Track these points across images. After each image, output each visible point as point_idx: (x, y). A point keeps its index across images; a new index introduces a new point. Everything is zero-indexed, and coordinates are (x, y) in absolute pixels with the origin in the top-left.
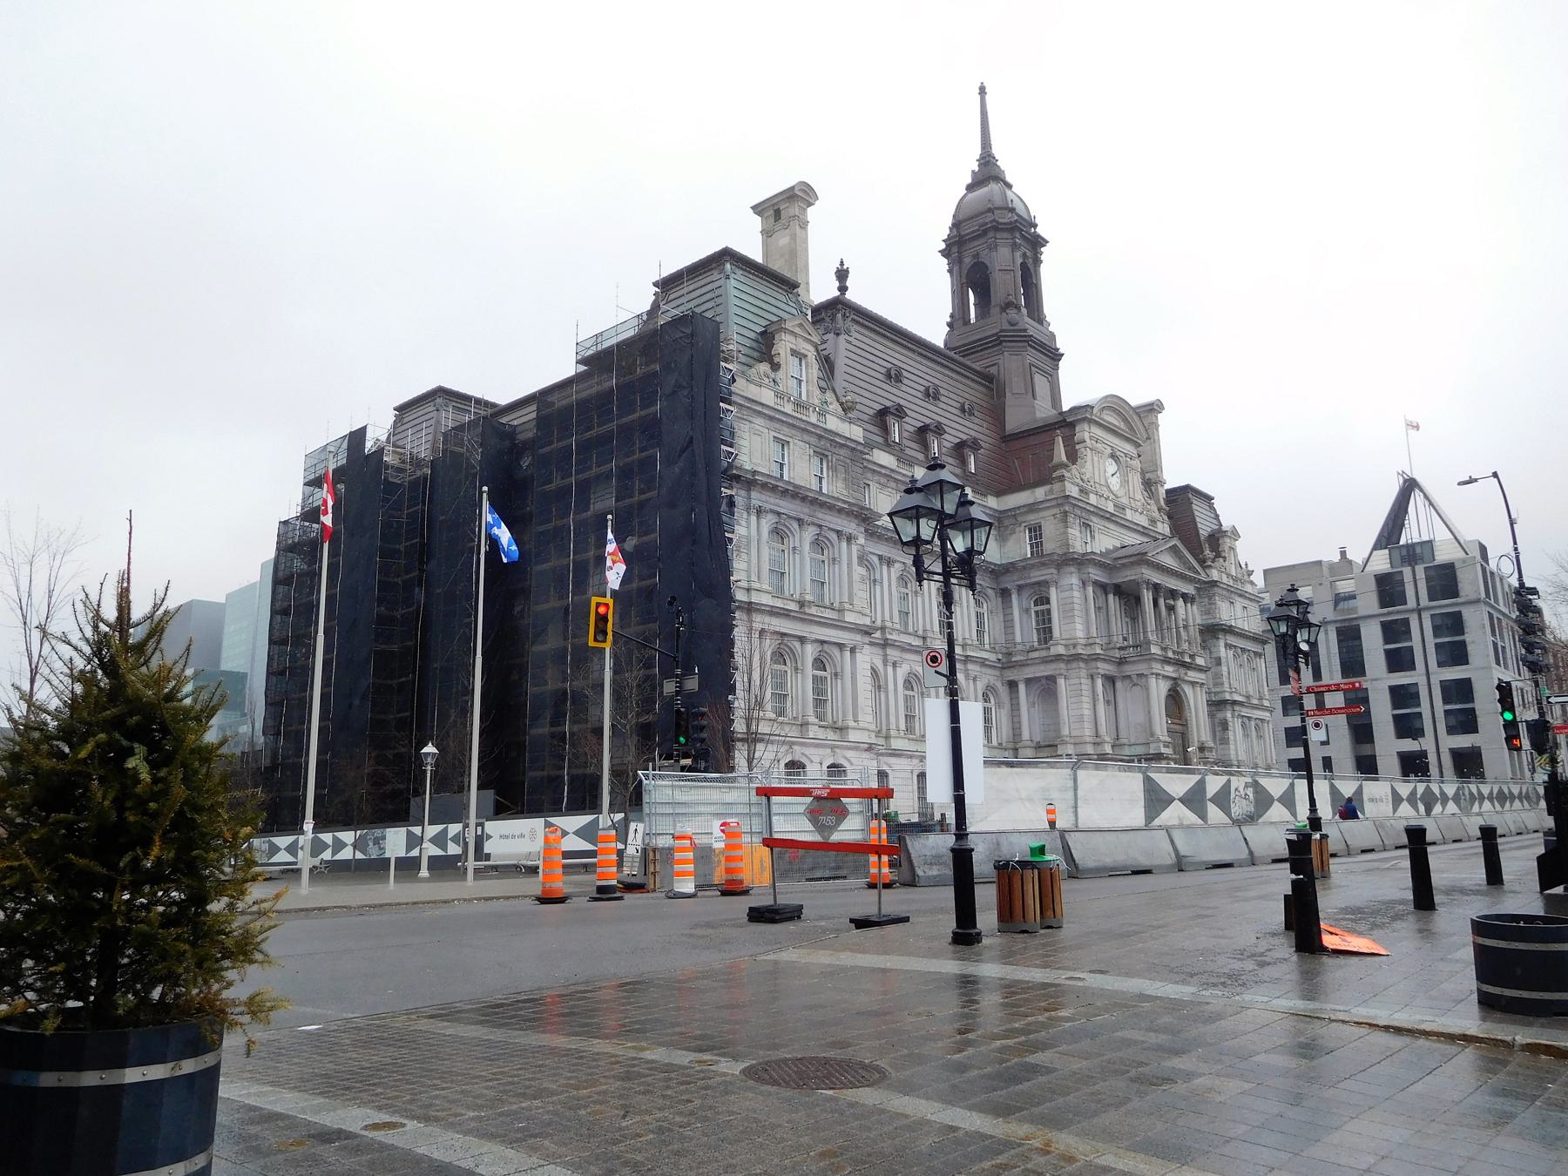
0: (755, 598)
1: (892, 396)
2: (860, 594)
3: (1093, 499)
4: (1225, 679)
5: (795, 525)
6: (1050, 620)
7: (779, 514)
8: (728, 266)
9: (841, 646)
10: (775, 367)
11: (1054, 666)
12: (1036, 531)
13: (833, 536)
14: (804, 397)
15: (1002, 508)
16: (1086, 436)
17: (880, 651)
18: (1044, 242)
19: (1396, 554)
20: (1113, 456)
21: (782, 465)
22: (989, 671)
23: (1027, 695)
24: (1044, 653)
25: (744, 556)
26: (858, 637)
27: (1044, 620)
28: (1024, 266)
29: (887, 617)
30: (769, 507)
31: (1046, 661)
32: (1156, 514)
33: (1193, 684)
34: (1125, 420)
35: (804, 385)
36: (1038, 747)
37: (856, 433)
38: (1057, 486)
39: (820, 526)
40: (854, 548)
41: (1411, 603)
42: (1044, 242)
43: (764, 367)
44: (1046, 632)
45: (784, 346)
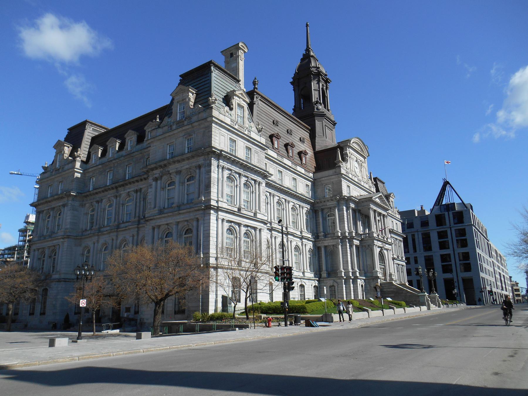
0: (220, 204)
1: (275, 130)
3: (350, 176)
5: (238, 175)
8: (212, 68)
9: (255, 229)
10: (231, 109)
16: (348, 152)
26: (262, 225)
28: (322, 89)
32: (371, 184)
33: (387, 250)
34: (361, 148)
37: (263, 140)
38: (337, 170)
39: (248, 177)
43: (227, 108)
45: (235, 101)
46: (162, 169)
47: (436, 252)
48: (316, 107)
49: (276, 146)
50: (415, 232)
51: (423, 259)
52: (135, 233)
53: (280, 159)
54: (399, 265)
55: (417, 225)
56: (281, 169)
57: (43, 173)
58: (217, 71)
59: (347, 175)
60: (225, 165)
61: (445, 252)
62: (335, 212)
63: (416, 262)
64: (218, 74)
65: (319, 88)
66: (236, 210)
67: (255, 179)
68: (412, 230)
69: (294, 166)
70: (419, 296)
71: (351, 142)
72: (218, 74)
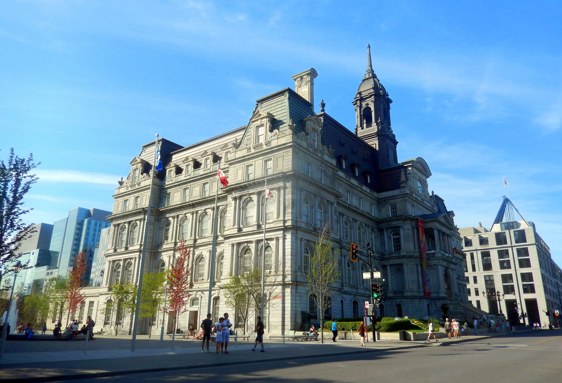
7: (308, 191)
11: (402, 260)
12: (394, 208)
15: (380, 197)
18: (391, 101)
19: (503, 226)
20: (420, 180)
21: (308, 172)
22: (376, 261)
23: (391, 271)
24: (398, 255)
27: (397, 242)
31: (399, 257)
33: (452, 269)
34: (424, 167)
35: (316, 142)
36: (395, 292)
38: (402, 190)
39: (322, 198)
41: (509, 244)
42: (391, 101)
43: (303, 133)
44: (398, 247)
47: (497, 272)
54: (460, 284)
61: (506, 272)
66: (312, 229)
67: (328, 199)
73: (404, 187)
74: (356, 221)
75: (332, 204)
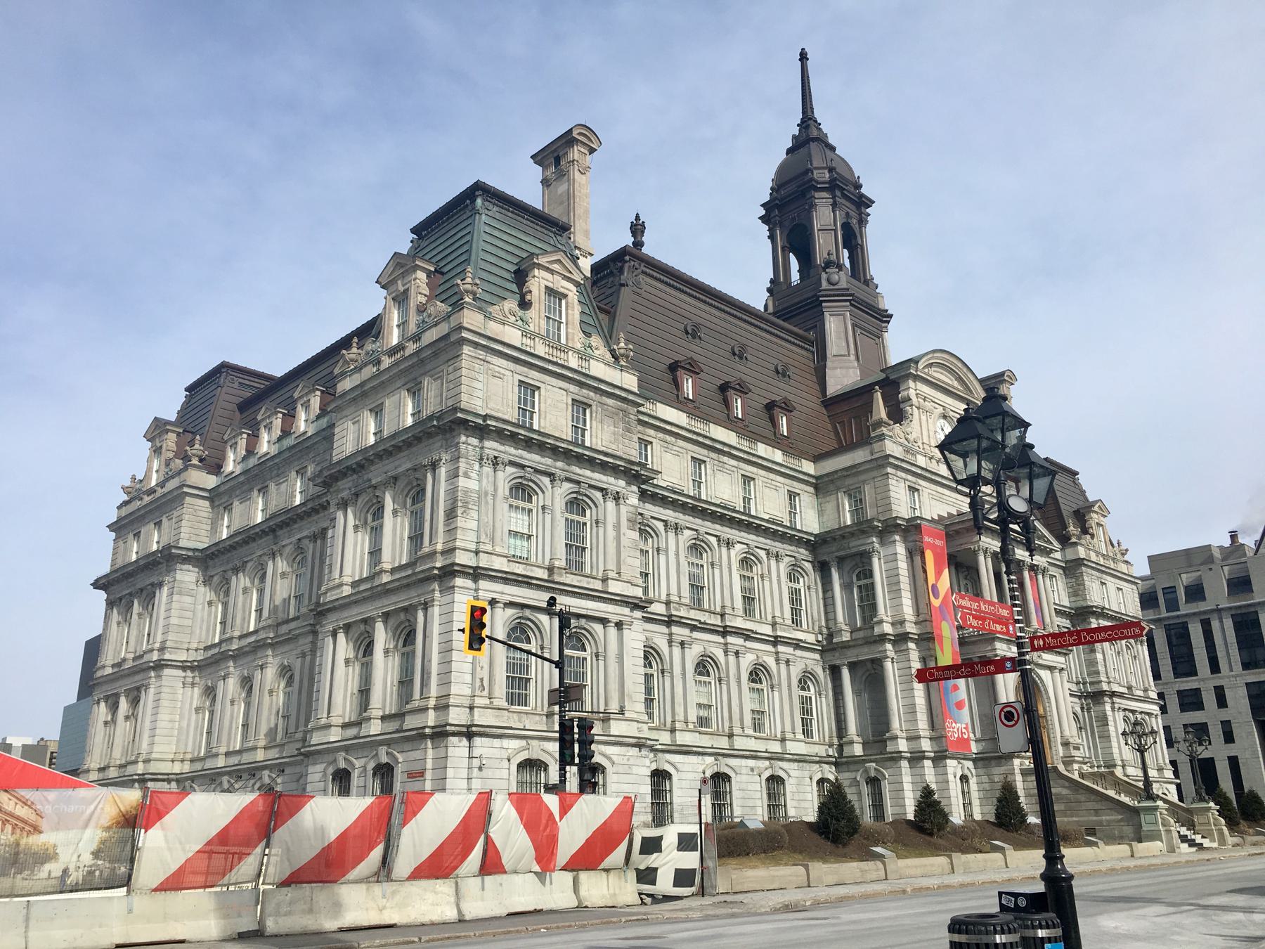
0: (484, 561)
2: (630, 561)
4: (1101, 668)
5: (546, 480)
6: (874, 596)
7: (523, 467)
8: (479, 201)
9: (604, 621)
10: (524, 304)
13: (598, 495)
14: (563, 341)
16: (912, 393)
17: (664, 629)
18: (869, 203)
20: (945, 417)
24: (868, 633)
25: (475, 515)
26: (626, 611)
28: (846, 227)
29: (674, 590)
30: (507, 458)
33: (1051, 668)
34: (959, 379)
35: (563, 327)
38: (876, 446)
39: (578, 483)
40: (623, 509)
42: (869, 203)
43: (511, 304)
46: (355, 476)
48: (824, 276)
49: (688, 387)
50: (1212, 611)
51: (1243, 692)
52: (307, 648)
53: (698, 426)
55: (1218, 594)
56: (701, 453)
57: (125, 503)
58: (496, 209)
59: (909, 458)
60: (502, 455)
62: (870, 564)
63: (1222, 702)
64: (498, 216)
65: (835, 224)
67: (604, 486)
68: (1202, 606)
69: (745, 445)
70: (1135, 811)
71: (921, 366)
72: (498, 216)
73: (881, 437)
74: (729, 544)
75: (617, 498)
